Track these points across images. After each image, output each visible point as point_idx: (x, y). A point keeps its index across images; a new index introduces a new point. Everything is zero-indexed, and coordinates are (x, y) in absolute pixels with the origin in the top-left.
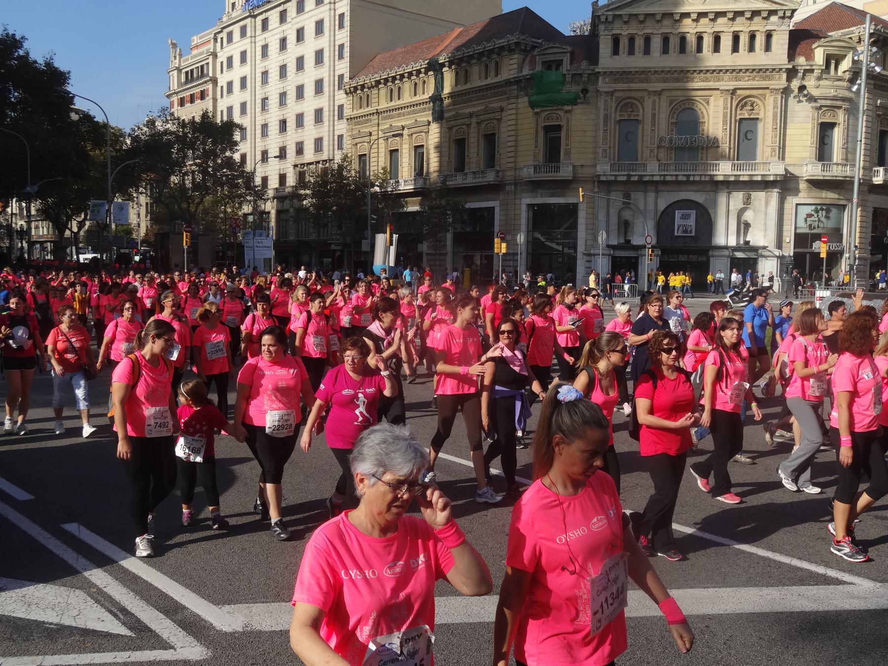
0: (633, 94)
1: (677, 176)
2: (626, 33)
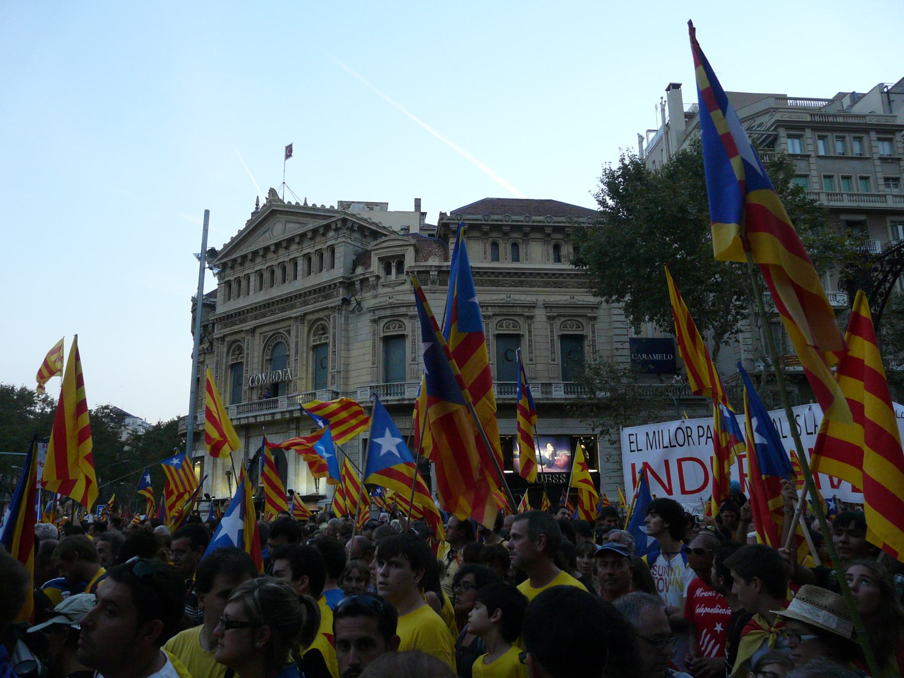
0: (238, 337)
1: (248, 417)
2: (232, 278)
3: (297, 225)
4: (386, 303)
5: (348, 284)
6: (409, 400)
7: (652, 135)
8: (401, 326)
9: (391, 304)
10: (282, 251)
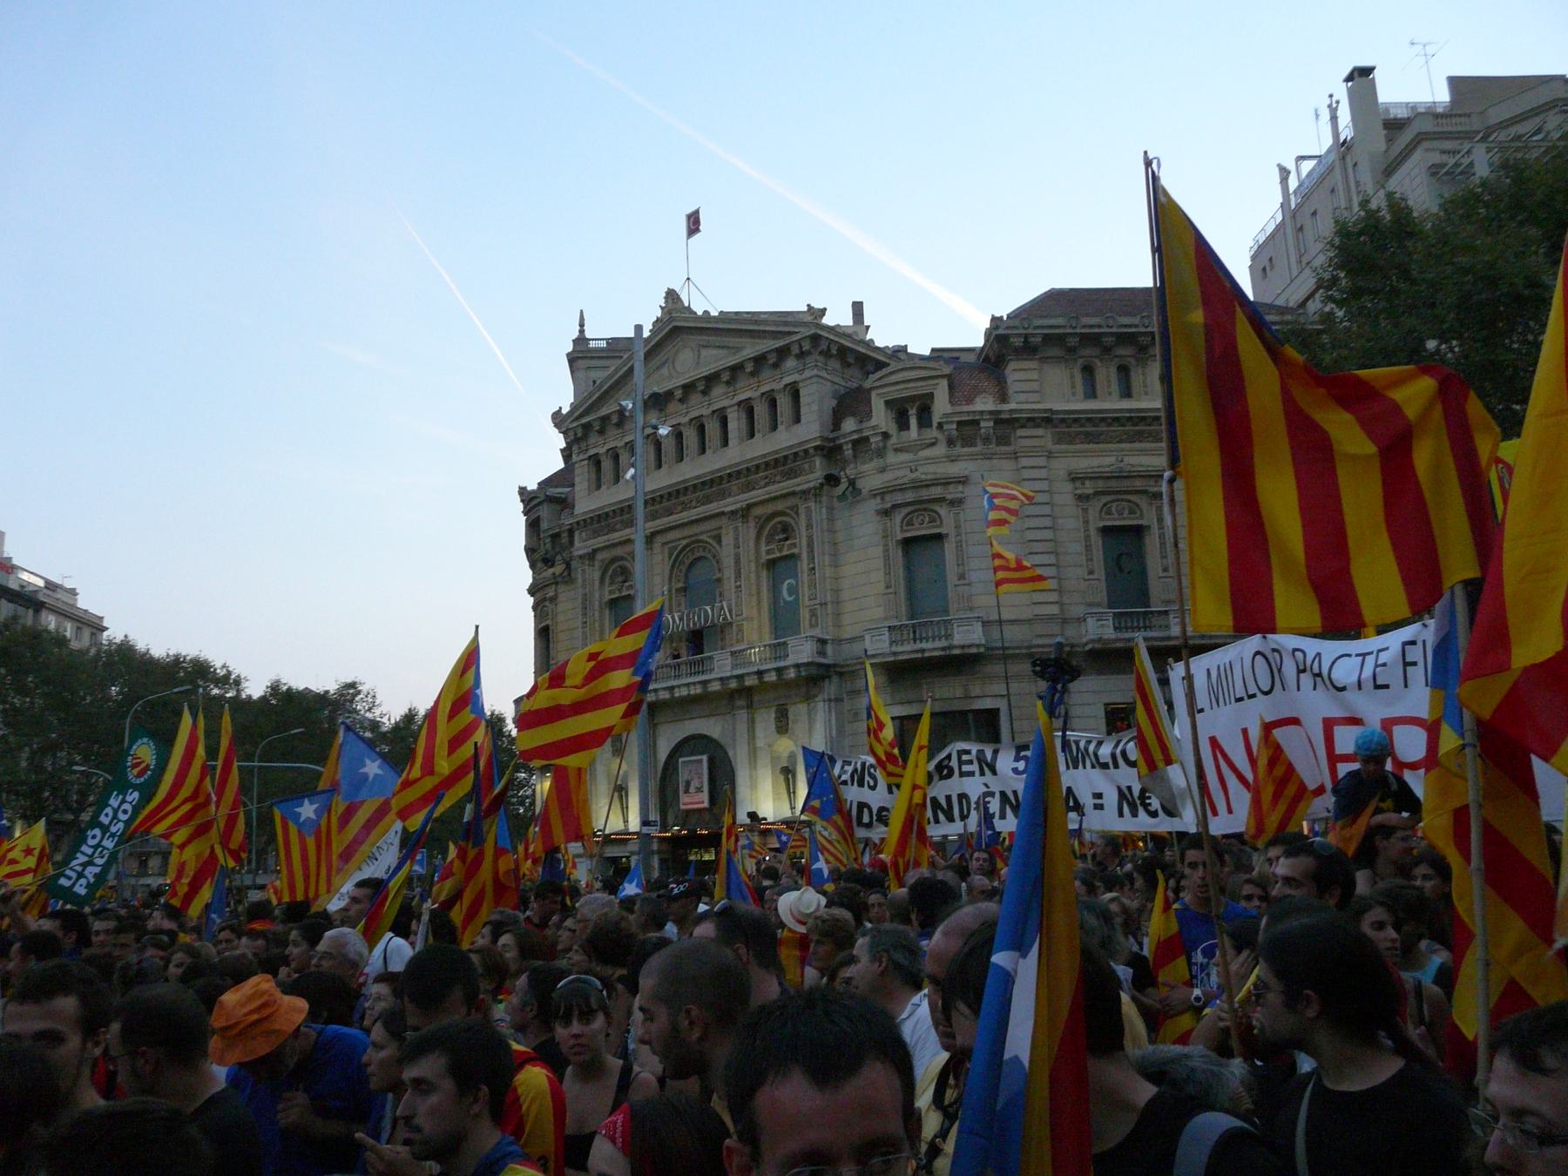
0: (619, 551)
3: (722, 352)
4: (905, 480)
5: (830, 450)
6: (963, 647)
7: (1307, 166)
8: (935, 519)
9: (914, 481)
10: (695, 398)
